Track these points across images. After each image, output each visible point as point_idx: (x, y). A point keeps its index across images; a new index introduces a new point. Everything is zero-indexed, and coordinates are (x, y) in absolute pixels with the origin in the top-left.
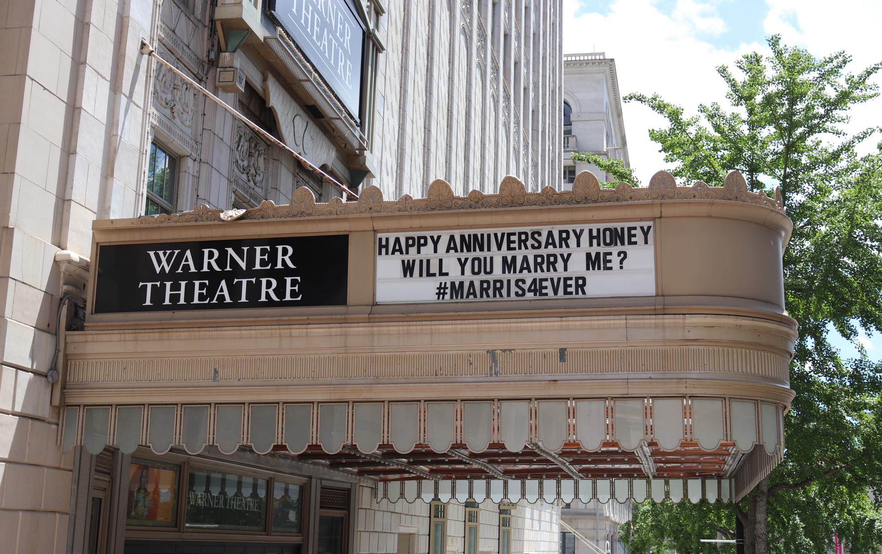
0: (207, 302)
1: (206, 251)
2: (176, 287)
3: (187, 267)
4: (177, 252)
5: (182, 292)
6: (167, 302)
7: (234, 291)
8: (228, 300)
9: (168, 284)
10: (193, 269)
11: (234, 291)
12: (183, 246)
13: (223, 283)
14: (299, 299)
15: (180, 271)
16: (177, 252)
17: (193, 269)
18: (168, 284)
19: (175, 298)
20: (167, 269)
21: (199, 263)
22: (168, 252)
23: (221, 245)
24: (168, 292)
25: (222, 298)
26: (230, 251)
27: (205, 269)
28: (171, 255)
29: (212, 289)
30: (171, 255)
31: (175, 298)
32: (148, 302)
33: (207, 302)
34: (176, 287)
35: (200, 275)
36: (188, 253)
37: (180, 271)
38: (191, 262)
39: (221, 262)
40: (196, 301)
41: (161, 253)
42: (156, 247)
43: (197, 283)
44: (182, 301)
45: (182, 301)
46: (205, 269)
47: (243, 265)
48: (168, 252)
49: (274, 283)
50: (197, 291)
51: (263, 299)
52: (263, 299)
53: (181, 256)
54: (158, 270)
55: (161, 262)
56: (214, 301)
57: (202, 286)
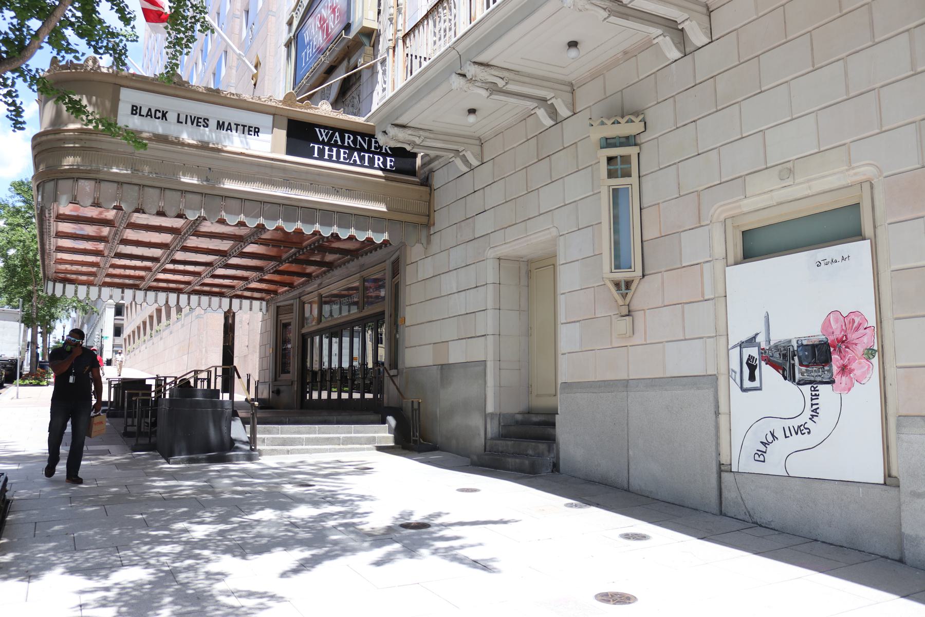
3: (336, 141)
5: (334, 154)
6: (326, 157)
7: (362, 159)
8: (358, 163)
9: (327, 148)
10: (339, 143)
11: (362, 159)
12: (335, 129)
13: (356, 154)
17: (339, 143)
18: (327, 148)
19: (330, 156)
21: (343, 140)
23: (355, 134)
24: (327, 152)
25: (355, 161)
26: (359, 138)
27: (346, 144)
31: (330, 156)
35: (343, 147)
36: (337, 134)
38: (338, 139)
39: (355, 141)
40: (342, 160)
43: (342, 151)
44: (334, 158)
45: (334, 158)
46: (346, 144)
47: (366, 147)
49: (382, 159)
52: (376, 165)
53: (333, 135)
55: (323, 135)
57: (345, 153)
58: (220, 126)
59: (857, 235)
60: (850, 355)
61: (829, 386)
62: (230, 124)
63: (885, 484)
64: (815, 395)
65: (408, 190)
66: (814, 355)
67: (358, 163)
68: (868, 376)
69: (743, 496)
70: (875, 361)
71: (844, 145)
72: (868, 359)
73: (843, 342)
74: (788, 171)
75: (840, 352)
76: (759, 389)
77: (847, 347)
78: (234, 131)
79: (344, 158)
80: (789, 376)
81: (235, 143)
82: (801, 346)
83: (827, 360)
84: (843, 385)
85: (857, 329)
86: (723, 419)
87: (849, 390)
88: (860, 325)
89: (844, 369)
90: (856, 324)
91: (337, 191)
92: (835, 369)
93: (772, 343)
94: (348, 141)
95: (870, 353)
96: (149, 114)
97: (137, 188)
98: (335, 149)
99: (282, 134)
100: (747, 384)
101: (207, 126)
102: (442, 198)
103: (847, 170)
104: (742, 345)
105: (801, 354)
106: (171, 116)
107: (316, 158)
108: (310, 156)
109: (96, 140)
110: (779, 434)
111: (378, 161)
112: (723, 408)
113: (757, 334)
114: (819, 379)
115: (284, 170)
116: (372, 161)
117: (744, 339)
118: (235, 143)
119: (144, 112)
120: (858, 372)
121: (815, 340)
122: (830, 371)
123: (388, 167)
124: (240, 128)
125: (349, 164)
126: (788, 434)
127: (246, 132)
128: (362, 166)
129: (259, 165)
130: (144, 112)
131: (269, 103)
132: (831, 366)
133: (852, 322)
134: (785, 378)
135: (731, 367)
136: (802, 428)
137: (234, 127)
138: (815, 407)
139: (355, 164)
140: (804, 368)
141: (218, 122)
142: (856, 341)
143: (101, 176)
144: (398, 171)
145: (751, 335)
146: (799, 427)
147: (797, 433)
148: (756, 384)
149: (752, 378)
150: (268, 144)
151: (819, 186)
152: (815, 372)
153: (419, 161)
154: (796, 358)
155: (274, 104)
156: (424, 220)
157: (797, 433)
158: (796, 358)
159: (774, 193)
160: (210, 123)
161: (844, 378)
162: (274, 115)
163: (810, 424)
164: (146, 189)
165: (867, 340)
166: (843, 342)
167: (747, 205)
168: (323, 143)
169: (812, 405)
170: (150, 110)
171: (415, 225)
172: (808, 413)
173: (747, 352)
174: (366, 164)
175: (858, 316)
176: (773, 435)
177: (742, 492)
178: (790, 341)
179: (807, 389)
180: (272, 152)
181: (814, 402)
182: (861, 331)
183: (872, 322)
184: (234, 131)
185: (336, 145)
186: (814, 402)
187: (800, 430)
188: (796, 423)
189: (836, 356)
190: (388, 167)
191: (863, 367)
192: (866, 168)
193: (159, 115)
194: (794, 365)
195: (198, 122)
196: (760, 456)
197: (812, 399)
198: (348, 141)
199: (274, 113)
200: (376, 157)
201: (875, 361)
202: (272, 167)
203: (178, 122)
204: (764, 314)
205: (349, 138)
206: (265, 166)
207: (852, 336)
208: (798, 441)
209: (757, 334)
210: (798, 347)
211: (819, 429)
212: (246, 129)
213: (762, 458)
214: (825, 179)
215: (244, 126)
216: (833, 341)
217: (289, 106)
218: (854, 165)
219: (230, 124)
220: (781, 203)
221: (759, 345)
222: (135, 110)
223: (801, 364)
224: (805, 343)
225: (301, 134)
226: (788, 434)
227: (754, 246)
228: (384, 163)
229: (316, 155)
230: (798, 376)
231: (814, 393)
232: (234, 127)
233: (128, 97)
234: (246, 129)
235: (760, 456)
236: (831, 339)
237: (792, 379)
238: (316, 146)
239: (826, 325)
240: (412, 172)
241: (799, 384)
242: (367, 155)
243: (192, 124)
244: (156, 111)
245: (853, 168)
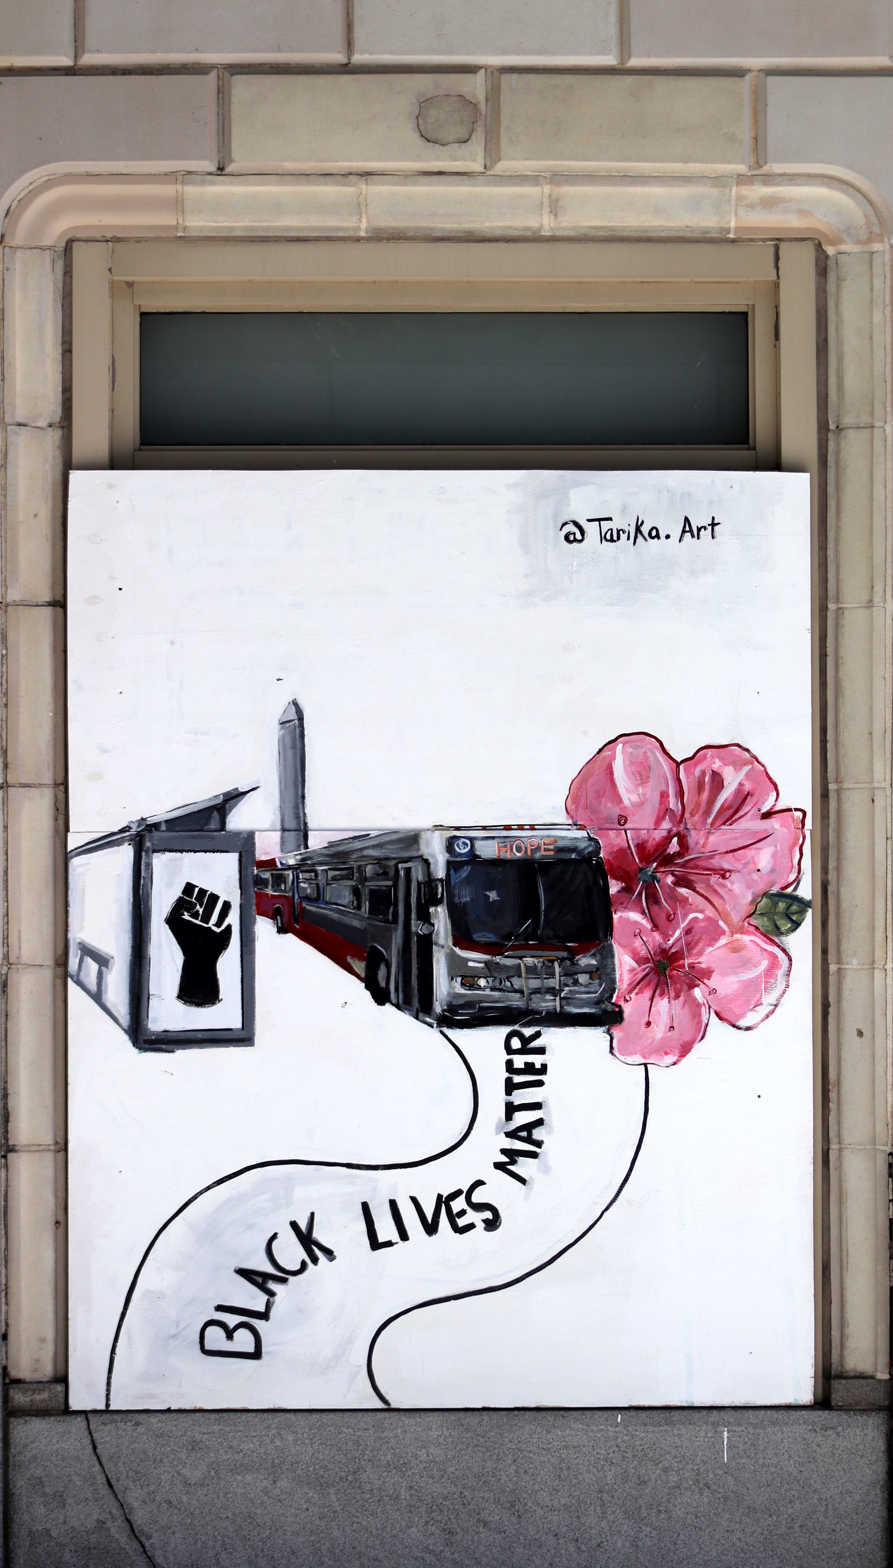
59: (727, 435)
60: (698, 912)
61: (595, 1036)
63: (823, 1401)
64: (529, 1068)
66: (528, 906)
68: (769, 999)
69: (140, 1518)
70: (801, 942)
71: (738, 73)
72: (773, 934)
73: (667, 860)
74: (462, 107)
75: (653, 898)
76: (242, 1037)
77: (689, 885)
80: (400, 982)
82: (466, 862)
83: (595, 931)
84: (659, 1031)
85: (732, 813)
86: (29, 1175)
87: (685, 1049)
88: (742, 798)
89: (667, 971)
90: (726, 794)
92: (624, 964)
93: (316, 842)
95: (778, 911)
100: (168, 1012)
103: (741, 180)
104: (145, 839)
105: (465, 897)
110: (341, 1231)
112: (29, 1122)
113: (234, 797)
114: (548, 1003)
117: (159, 808)
120: (725, 984)
121: (537, 843)
122: (604, 972)
126: (386, 1230)
132: (607, 955)
133: (712, 787)
134: (381, 997)
135: (77, 934)
136: (458, 1204)
138: (522, 1118)
140: (475, 959)
142: (725, 863)
145: (200, 792)
146: (444, 1201)
147: (431, 1228)
148: (225, 1014)
149: (199, 987)
151: (591, 208)
152: (528, 973)
154: (440, 916)
157: (431, 1228)
158: (440, 916)
159: (376, 190)
161: (662, 1005)
163: (497, 1189)
165: (775, 859)
166: (667, 860)
167: (219, 204)
169: (511, 1110)
172: (490, 1140)
173: (172, 874)
175: (738, 765)
176: (306, 1239)
177: (134, 1497)
178: (413, 839)
179: (487, 1045)
181: (520, 1097)
182: (748, 824)
183: (796, 789)
186: (520, 1097)
187: (446, 1214)
188: (429, 1184)
189: (634, 916)
191: (747, 963)
192: (821, 191)
194: (426, 943)
196: (236, 1332)
197: (510, 1087)
201: (801, 942)
204: (278, 709)
207: (709, 841)
208: (433, 1260)
209: (234, 797)
210: (451, 865)
211: (535, 1209)
213: (243, 1341)
214: (646, 190)
216: (623, 852)
218: (777, 168)
220: (396, 237)
221: (245, 844)
223: (463, 937)
224: (488, 850)
226: (386, 1230)
227: (229, 393)
230: (444, 987)
231: (519, 1061)
235: (236, 1332)
236: (611, 842)
237: (416, 999)
239: (592, 784)
241: (450, 1019)
245: (769, 179)
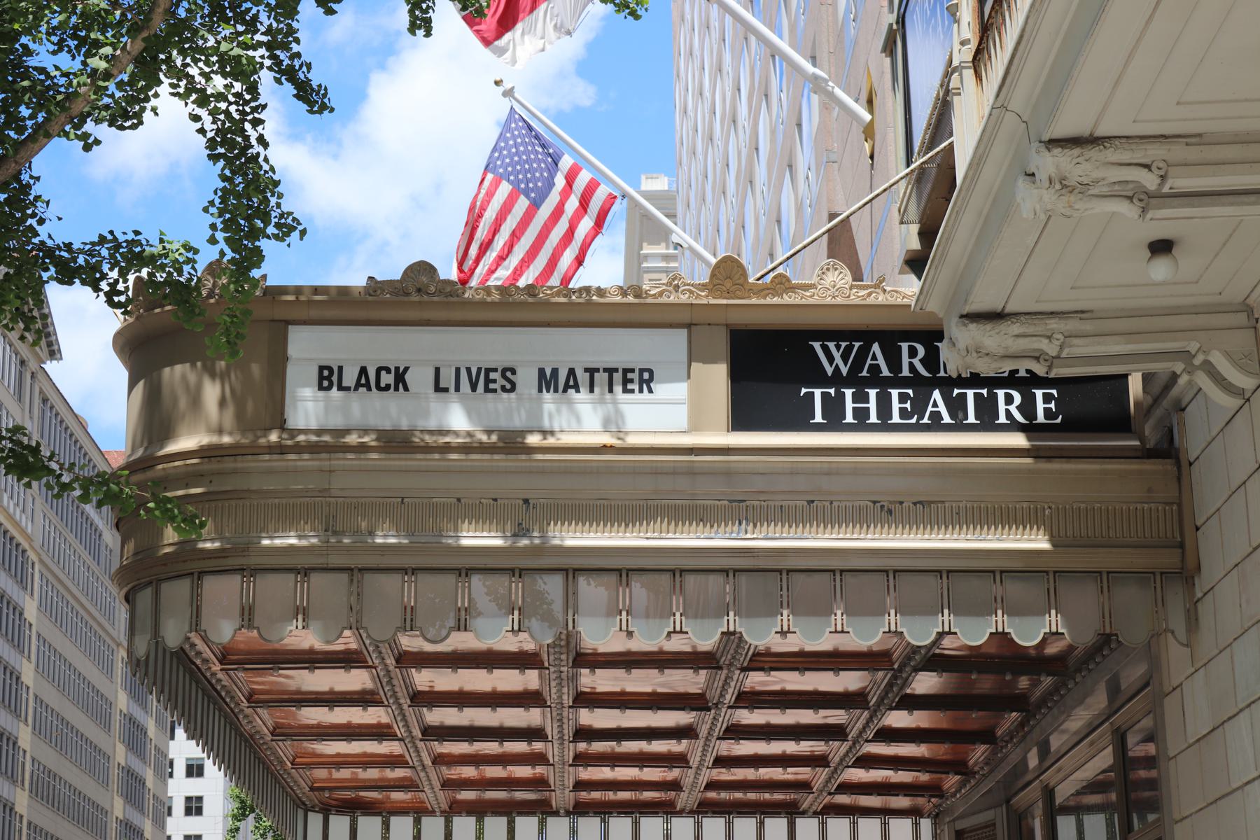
0: (914, 421)
1: (905, 346)
2: (860, 397)
3: (875, 369)
4: (857, 345)
5: (872, 405)
6: (849, 418)
7: (956, 406)
8: (947, 419)
9: (848, 393)
10: (886, 372)
12: (867, 336)
14: (1059, 420)
15: (864, 373)
16: (857, 345)
17: (886, 372)
18: (848, 393)
19: (861, 414)
20: (844, 370)
21: (894, 361)
22: (844, 344)
24: (849, 405)
25: (936, 416)
27: (906, 372)
28: (849, 349)
29: (920, 405)
30: (849, 349)
31: (861, 414)
32: (818, 418)
33: (914, 421)
34: (860, 397)
36: (876, 348)
37: (864, 373)
38: (881, 361)
40: (896, 419)
41: (831, 345)
42: (826, 335)
43: (895, 393)
44: (873, 418)
45: (873, 418)
46: (906, 372)
48: (844, 344)
50: (896, 405)
51: (1002, 419)
52: (1002, 419)
53: (864, 352)
54: (830, 370)
55: (834, 360)
56: (926, 420)
57: (903, 398)
58: (547, 381)
62: (572, 372)
65: (1105, 480)
67: (947, 419)
78: (584, 390)
79: (903, 413)
81: (580, 422)
91: (887, 512)
94: (911, 360)
96: (363, 379)
97: (344, 577)
98: (872, 393)
99: (717, 376)
101: (513, 389)
102: (1209, 487)
106: (419, 378)
107: (819, 428)
108: (802, 422)
109: (235, 472)
111: (1008, 405)
115: (728, 474)
116: (987, 410)
118: (580, 422)
119: (350, 378)
123: (1041, 417)
124: (601, 378)
125: (918, 428)
127: (618, 389)
128: (960, 426)
129: (656, 472)
130: (350, 378)
131: (673, 299)
137: (583, 377)
139: (936, 425)
141: (542, 372)
143: (254, 561)
144: (1072, 425)
150: (679, 411)
153: (1135, 386)
155: (684, 298)
156: (1169, 559)
160: (519, 379)
162: (689, 326)
164: (368, 577)
168: (838, 380)
170: (363, 371)
171: (1143, 576)
174: (972, 419)
180: (694, 427)
184: (584, 390)
185: (875, 379)
190: (1041, 417)
193: (387, 379)
195: (488, 381)
198: (911, 360)
199: (687, 321)
200: (1001, 394)
202: (692, 472)
203: (438, 389)
205: (913, 352)
206: (674, 472)
212: (618, 377)
215: (611, 371)
217: (729, 294)
219: (572, 372)
222: (327, 378)
225: (772, 363)
228: (1028, 407)
229: (818, 418)
232: (583, 377)
233: (307, 346)
234: (618, 377)
238: (818, 393)
240: (1120, 422)
242: (970, 394)
243: (474, 387)
244: (379, 370)
